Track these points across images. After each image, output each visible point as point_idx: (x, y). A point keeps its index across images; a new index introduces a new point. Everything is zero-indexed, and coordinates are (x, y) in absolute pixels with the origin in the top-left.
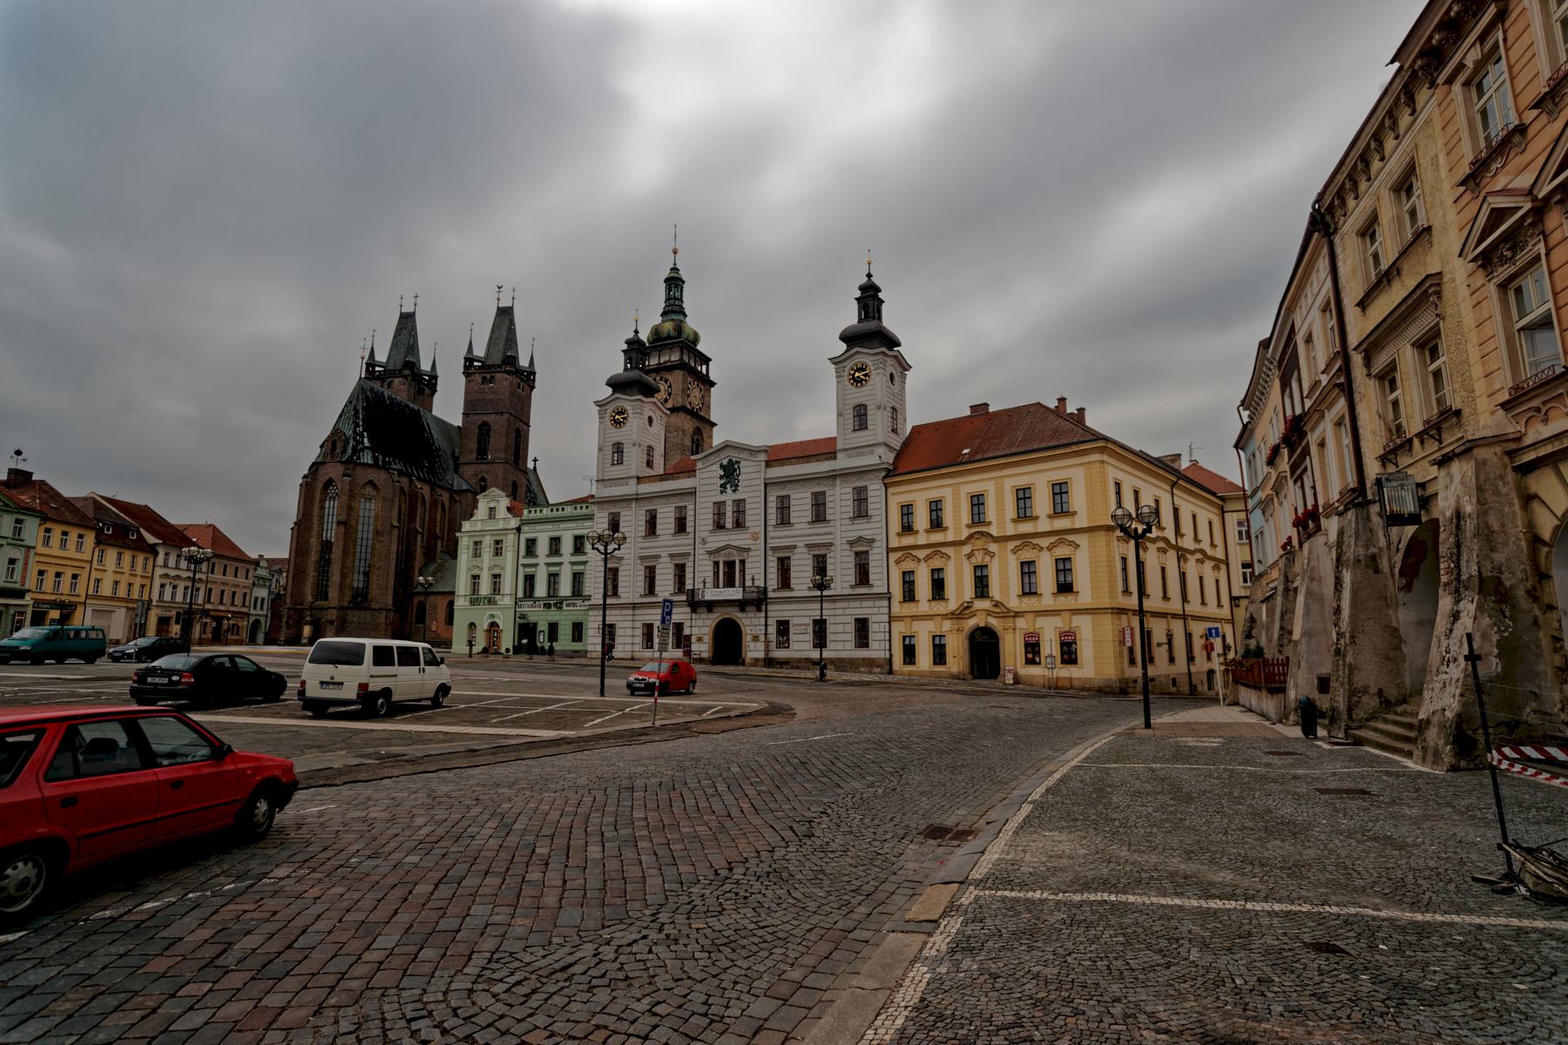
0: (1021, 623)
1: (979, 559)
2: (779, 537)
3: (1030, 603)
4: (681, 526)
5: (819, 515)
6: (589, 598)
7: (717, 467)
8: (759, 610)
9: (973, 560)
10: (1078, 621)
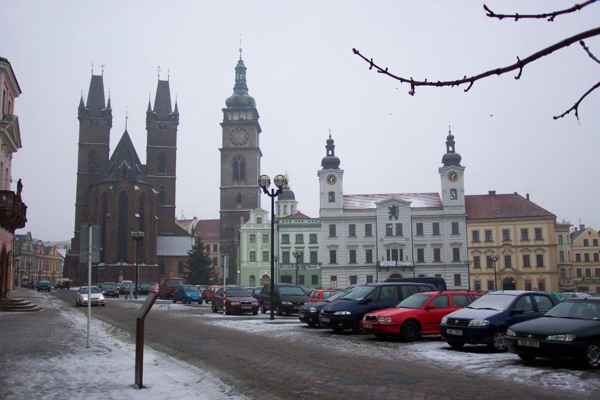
0: (524, 277)
1: (507, 253)
2: (419, 240)
3: (527, 270)
4: (368, 231)
5: (436, 231)
6: (320, 264)
7: (387, 208)
8: (412, 271)
9: (505, 254)
10: (545, 276)
